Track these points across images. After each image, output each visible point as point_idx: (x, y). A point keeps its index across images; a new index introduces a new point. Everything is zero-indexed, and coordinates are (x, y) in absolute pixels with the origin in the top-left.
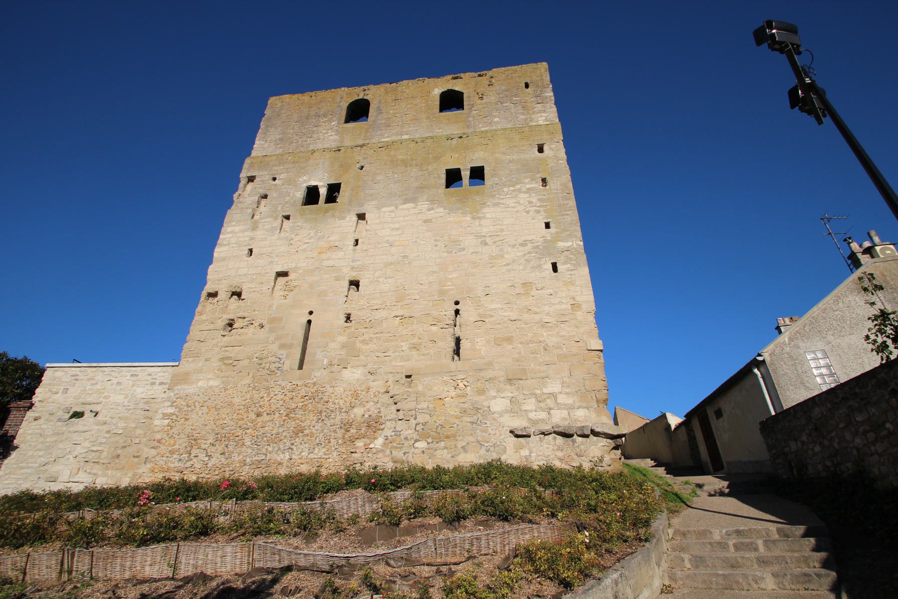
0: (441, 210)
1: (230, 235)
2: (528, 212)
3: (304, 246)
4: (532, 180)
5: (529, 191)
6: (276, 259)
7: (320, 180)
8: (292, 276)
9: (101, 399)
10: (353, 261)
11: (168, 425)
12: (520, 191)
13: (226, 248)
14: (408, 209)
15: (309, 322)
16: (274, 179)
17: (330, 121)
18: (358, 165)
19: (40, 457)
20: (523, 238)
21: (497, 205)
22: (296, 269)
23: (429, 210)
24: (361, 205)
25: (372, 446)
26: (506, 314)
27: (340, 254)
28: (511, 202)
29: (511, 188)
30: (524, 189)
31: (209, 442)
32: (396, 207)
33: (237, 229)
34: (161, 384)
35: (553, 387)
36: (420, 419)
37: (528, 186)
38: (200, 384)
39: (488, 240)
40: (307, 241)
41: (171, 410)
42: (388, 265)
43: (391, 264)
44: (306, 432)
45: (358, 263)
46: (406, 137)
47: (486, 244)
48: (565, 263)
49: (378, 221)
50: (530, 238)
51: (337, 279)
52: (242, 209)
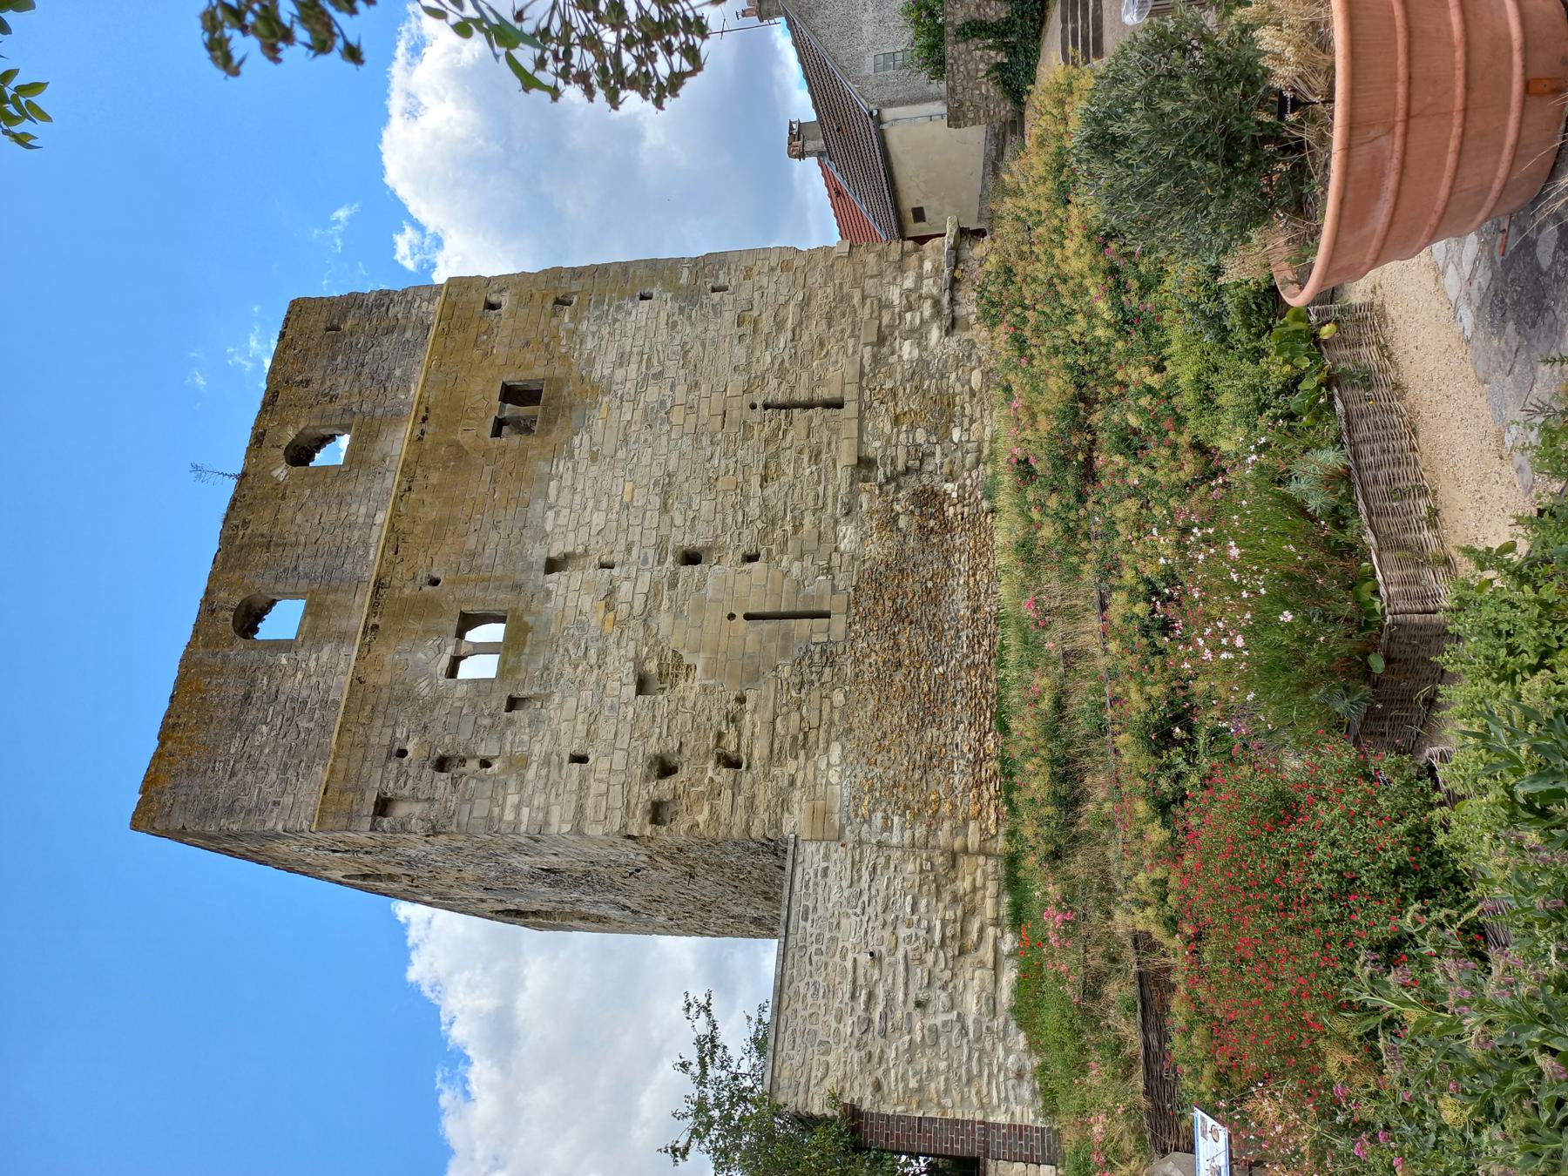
0: (577, 440)
1: (525, 811)
2: (616, 320)
3: (592, 652)
4: (554, 315)
5: (575, 318)
6: (608, 701)
7: (440, 650)
8: (652, 667)
9: (849, 964)
10: (645, 561)
11: (903, 815)
12: (572, 333)
13: (555, 811)
14: (559, 489)
15: (748, 617)
16: (403, 753)
17: (270, 670)
18: (428, 588)
19: (949, 1043)
20: (663, 326)
21: (591, 362)
22: (638, 661)
23: (571, 456)
24: (530, 566)
25: (954, 495)
26: (782, 345)
27: (626, 587)
28: (590, 344)
29: (564, 342)
30: (572, 326)
31: (935, 732)
32: (550, 508)
33: (512, 799)
34: (826, 857)
35: (894, 295)
36: (920, 436)
37: (566, 319)
38: (834, 779)
39: (652, 371)
40: (581, 654)
41: (878, 819)
42: (665, 508)
43: (665, 504)
44: (930, 584)
45: (651, 552)
46: (381, 517)
47: (661, 373)
48: (717, 277)
49: (571, 536)
50: (663, 316)
51: (673, 585)
52: (464, 801)
